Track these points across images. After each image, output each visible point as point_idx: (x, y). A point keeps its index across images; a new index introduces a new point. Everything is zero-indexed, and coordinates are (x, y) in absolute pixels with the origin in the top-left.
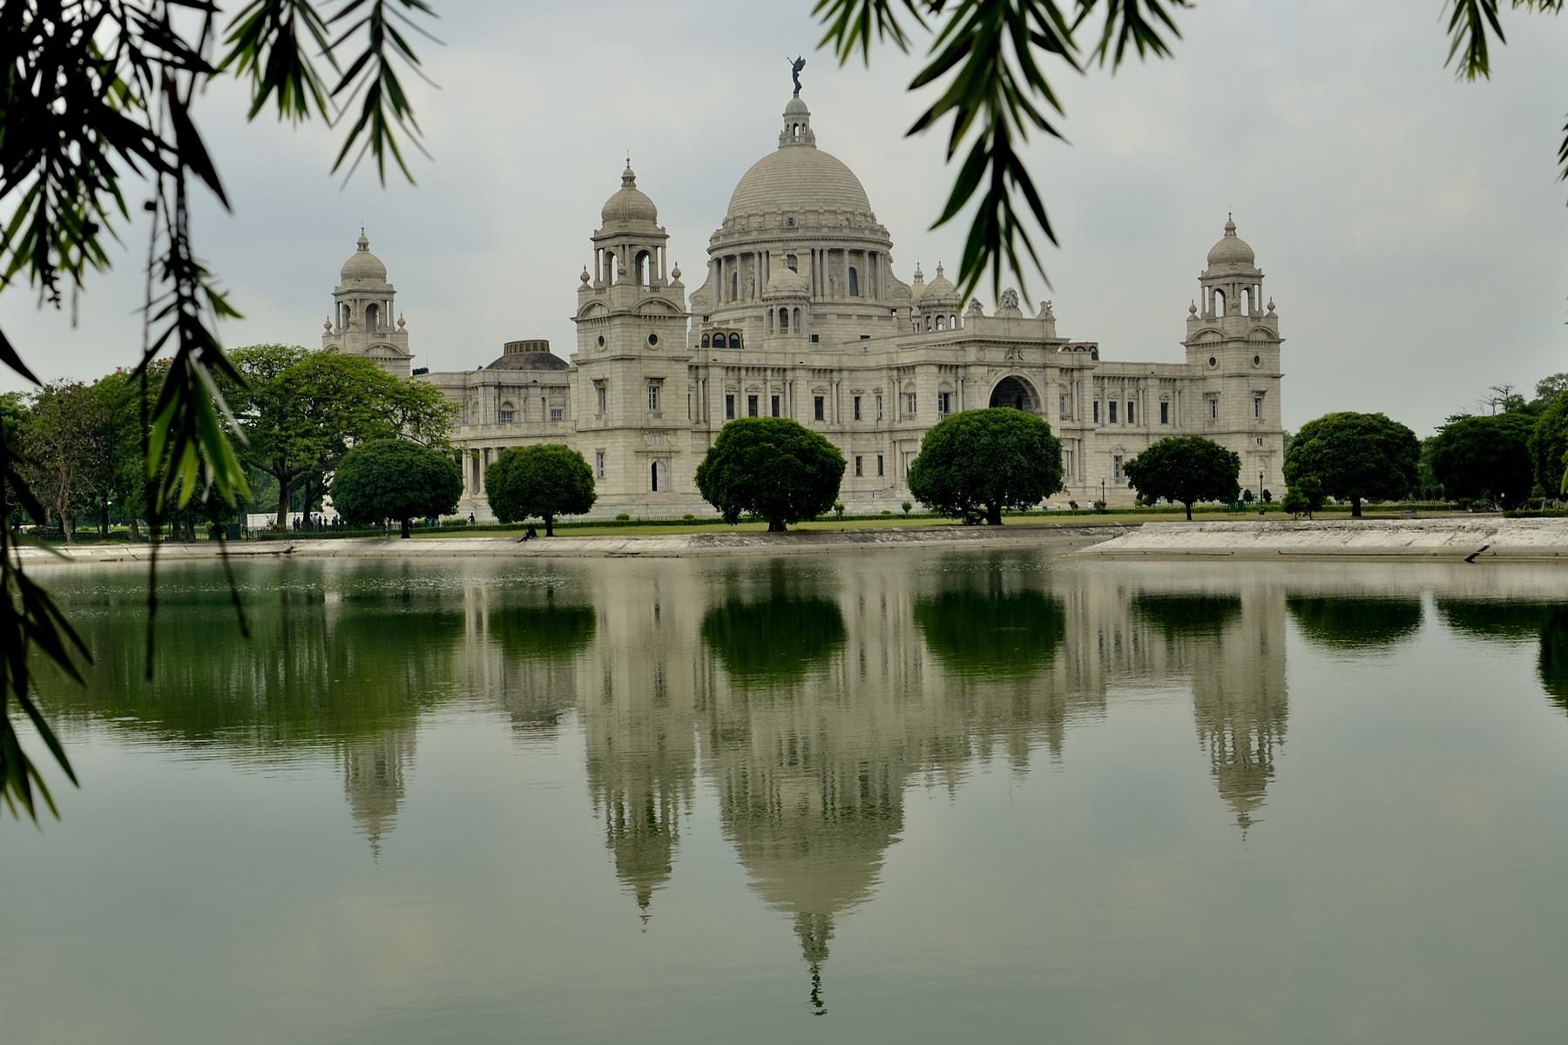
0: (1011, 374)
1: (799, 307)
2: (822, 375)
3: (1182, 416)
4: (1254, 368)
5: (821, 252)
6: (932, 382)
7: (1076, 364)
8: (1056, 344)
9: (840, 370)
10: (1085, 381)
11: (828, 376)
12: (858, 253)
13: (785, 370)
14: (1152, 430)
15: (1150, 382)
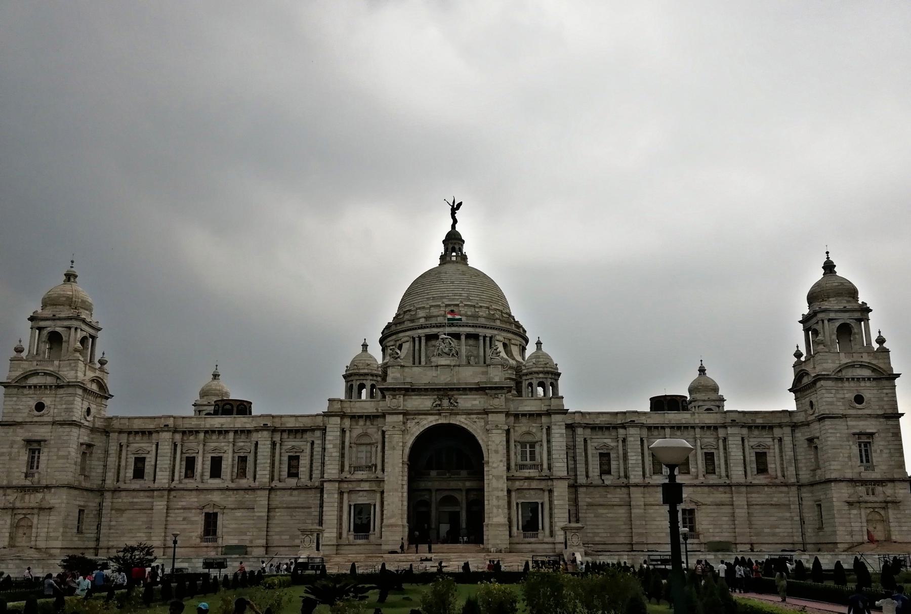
0: (440, 422)
1: (364, 382)
2: (299, 436)
3: (785, 467)
4: (854, 408)
5: (420, 338)
6: (335, 434)
7: (545, 408)
8: (496, 388)
9: (312, 430)
10: (553, 427)
11: (305, 436)
12: (457, 336)
13: (249, 432)
14: (734, 481)
15: (730, 431)
